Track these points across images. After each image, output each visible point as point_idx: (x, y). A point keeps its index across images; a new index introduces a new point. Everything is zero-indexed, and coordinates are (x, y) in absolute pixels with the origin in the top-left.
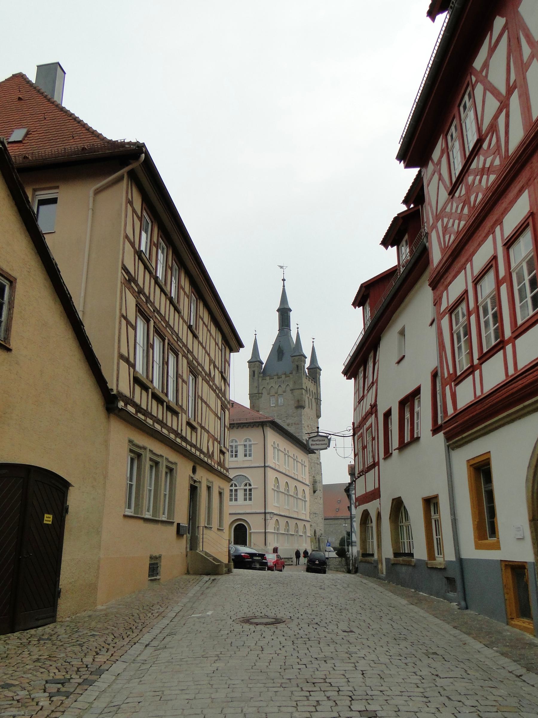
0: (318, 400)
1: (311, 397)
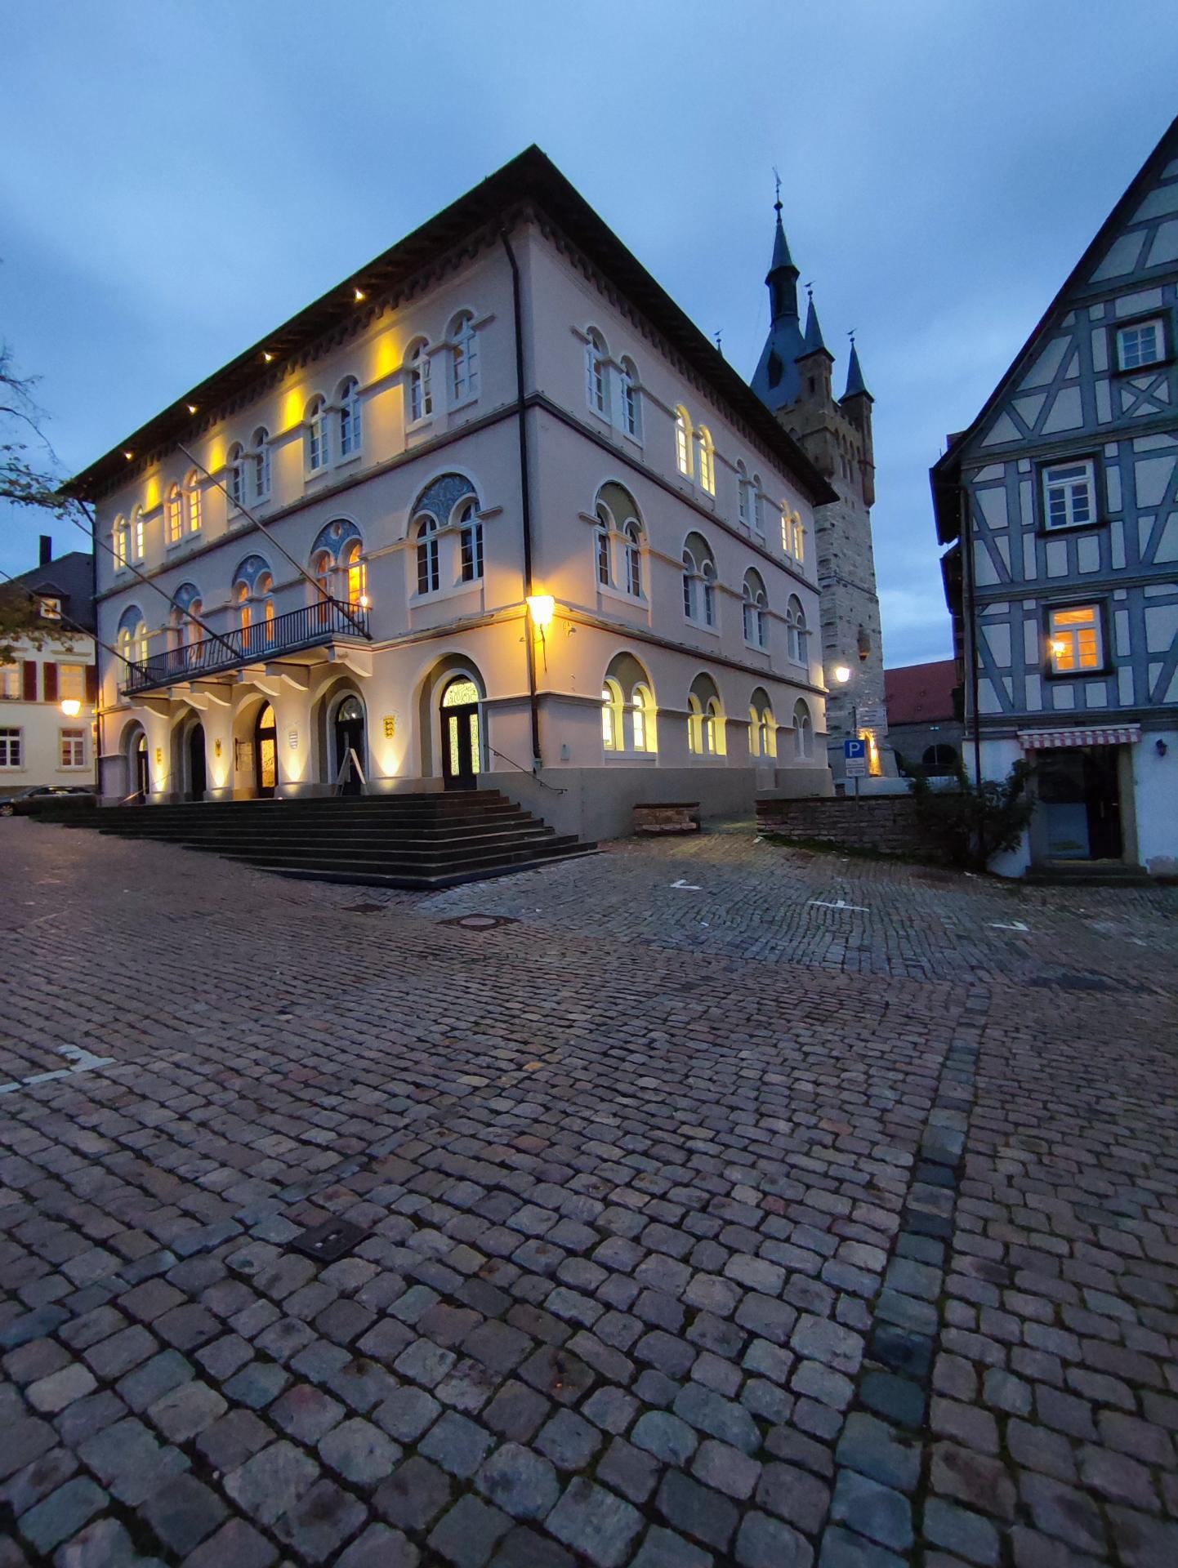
0: (866, 465)
1: (848, 457)
